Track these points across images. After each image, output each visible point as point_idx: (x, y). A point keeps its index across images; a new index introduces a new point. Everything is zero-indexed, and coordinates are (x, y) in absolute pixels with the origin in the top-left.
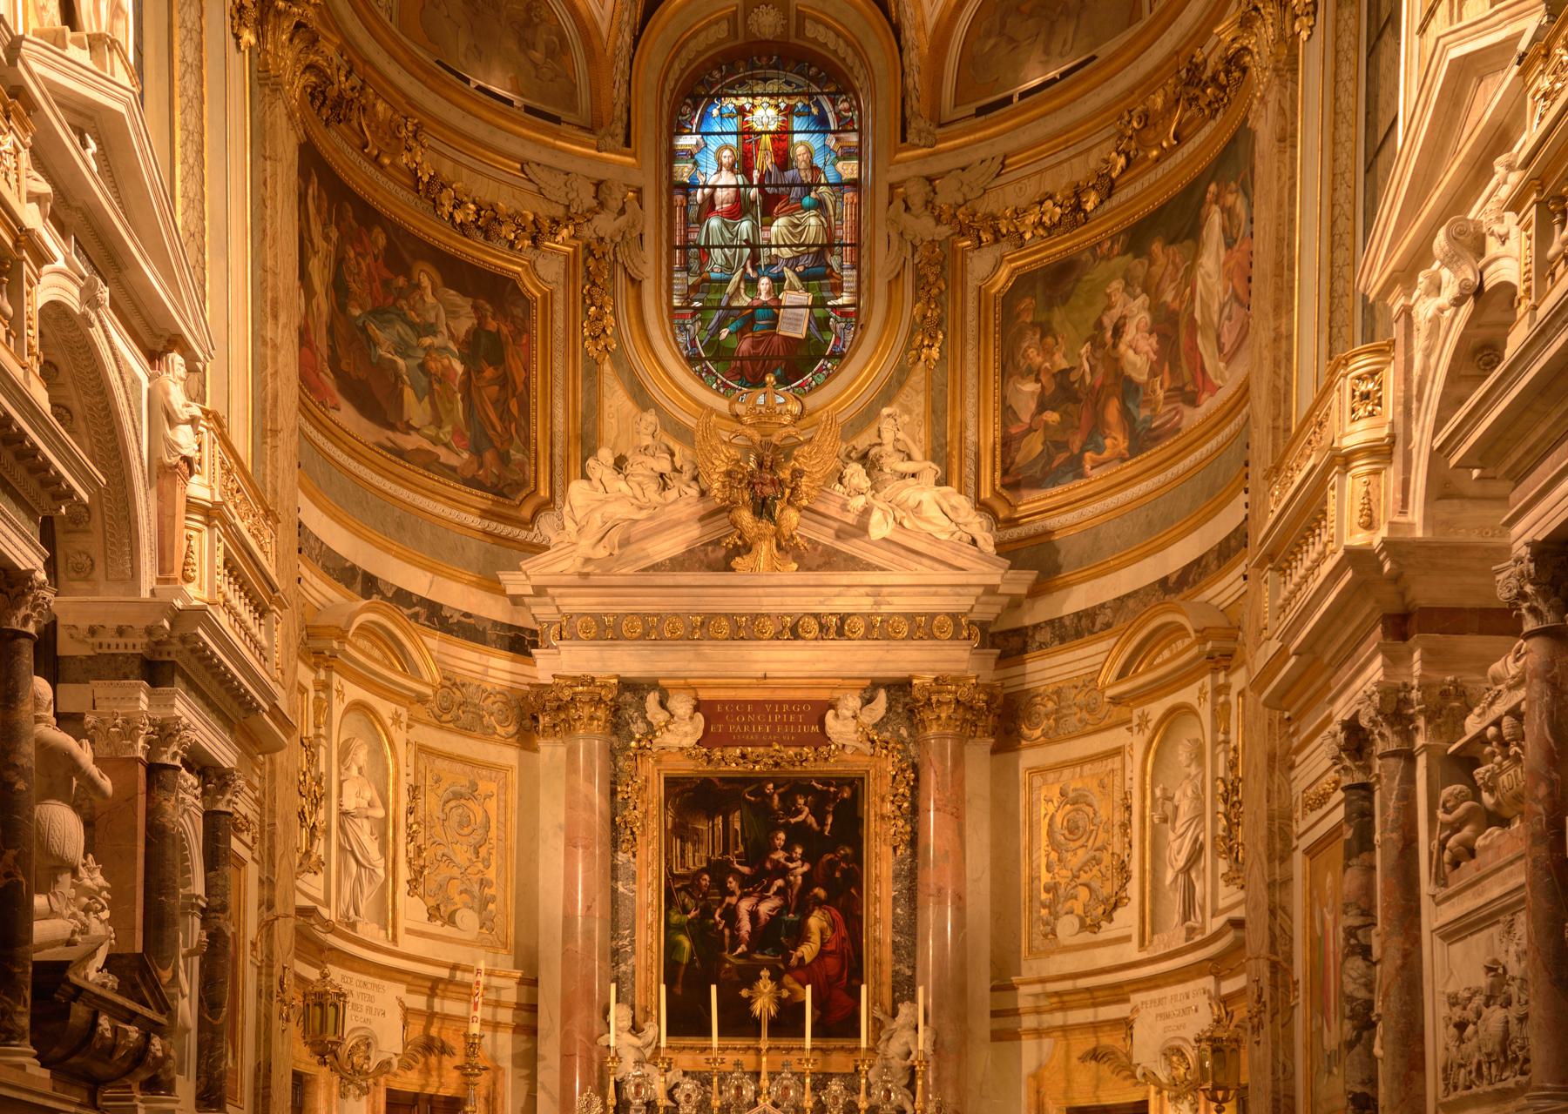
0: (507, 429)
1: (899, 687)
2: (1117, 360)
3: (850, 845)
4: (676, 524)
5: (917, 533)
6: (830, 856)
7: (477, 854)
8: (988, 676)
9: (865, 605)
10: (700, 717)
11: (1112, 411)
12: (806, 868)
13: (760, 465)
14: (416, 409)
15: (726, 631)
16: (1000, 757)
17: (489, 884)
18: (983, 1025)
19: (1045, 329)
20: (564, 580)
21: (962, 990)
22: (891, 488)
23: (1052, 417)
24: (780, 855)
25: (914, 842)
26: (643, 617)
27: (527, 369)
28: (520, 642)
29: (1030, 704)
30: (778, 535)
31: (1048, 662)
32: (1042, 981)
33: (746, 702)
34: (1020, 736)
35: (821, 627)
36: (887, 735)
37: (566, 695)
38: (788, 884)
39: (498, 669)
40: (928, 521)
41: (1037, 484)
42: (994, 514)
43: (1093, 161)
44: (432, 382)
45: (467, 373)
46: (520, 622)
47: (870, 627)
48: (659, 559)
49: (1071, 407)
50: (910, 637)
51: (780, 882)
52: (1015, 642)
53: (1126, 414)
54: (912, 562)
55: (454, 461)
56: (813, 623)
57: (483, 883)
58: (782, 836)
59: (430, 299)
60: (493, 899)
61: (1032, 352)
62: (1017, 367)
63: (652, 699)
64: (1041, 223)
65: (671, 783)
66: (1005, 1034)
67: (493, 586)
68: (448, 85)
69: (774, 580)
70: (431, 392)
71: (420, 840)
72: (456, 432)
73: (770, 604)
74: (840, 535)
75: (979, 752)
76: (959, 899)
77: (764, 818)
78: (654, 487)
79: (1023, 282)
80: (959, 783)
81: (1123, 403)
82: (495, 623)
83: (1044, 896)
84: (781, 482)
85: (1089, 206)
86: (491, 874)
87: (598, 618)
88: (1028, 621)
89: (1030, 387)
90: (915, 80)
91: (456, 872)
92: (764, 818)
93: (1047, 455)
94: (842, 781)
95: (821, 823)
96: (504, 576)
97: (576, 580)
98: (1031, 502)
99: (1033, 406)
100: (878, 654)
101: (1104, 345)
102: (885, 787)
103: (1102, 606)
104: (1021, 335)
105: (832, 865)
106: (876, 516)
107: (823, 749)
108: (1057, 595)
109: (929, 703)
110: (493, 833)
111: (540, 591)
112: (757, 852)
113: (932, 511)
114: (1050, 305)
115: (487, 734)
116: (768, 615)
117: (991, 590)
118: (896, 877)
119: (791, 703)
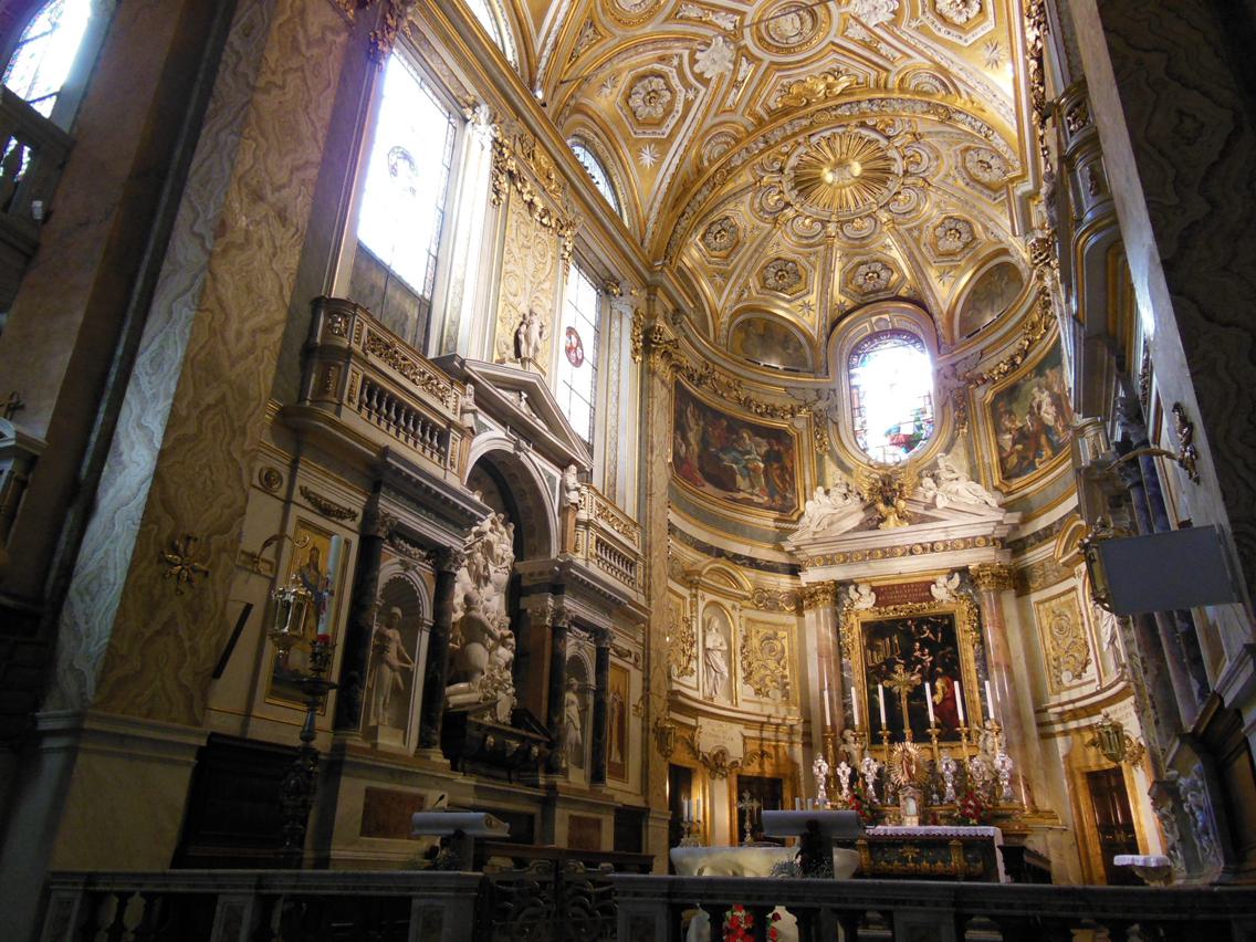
0: (784, 486)
1: (964, 571)
2: (1041, 419)
3: (950, 645)
4: (852, 513)
5: (959, 503)
6: (941, 652)
7: (779, 664)
8: (1007, 561)
9: (942, 537)
10: (873, 594)
11: (1043, 440)
12: (931, 658)
13: (884, 484)
14: (742, 482)
15: (880, 555)
16: (1020, 599)
17: (786, 677)
18: (1033, 731)
19: (1011, 413)
20: (806, 542)
21: (1018, 713)
22: (946, 486)
23: (1019, 447)
24: (918, 654)
25: (982, 641)
26: (843, 553)
27: (792, 462)
28: (794, 570)
29: (1028, 570)
30: (897, 511)
31: (1035, 552)
32: (1060, 705)
33: (893, 586)
34: (1029, 588)
35: (924, 549)
36: (962, 593)
37: (813, 590)
38: (923, 666)
39: (784, 583)
40: (963, 497)
41: (1017, 476)
42: (1001, 491)
43: (1017, 345)
44: (750, 472)
45: (766, 467)
46: (794, 562)
47: (946, 546)
48: (849, 528)
49: (1026, 442)
50: (965, 548)
51: (919, 666)
52: (1020, 544)
53: (1049, 441)
54: (961, 515)
55: (760, 501)
56: (919, 548)
57: (784, 677)
58: (918, 644)
59: (748, 441)
60: (787, 684)
61: (1007, 423)
62: (1001, 429)
63: (852, 588)
64: (1000, 373)
65: (863, 624)
66: (1046, 736)
67: (781, 549)
68: (749, 366)
69: (896, 531)
70: (749, 476)
71: (750, 659)
72: (762, 490)
73: (898, 541)
74: (926, 508)
75: (1009, 598)
76: (1009, 668)
77: (908, 637)
78: (841, 499)
79: (998, 396)
80: (1000, 611)
81: (1047, 436)
82: (783, 564)
83: (1055, 663)
84: (894, 490)
85: (1018, 362)
86: (787, 672)
87: (824, 556)
88: (1024, 534)
89: (1008, 436)
90: (941, 331)
91: (768, 672)
92: (908, 637)
93: (1020, 463)
94: (943, 616)
95: (936, 637)
96: (783, 544)
97: (811, 541)
98: (1016, 483)
99: (1010, 443)
100: (951, 557)
101: (1034, 414)
102: (965, 618)
103: (1054, 523)
104: (1001, 417)
105: (944, 656)
106: (939, 499)
107: (932, 603)
108: (1034, 522)
109: (978, 575)
110: (787, 654)
111: (798, 548)
112: (907, 654)
113: (963, 492)
114: (1011, 403)
115: (782, 610)
116: (898, 547)
117: (1000, 523)
118: (976, 660)
119: (914, 583)
